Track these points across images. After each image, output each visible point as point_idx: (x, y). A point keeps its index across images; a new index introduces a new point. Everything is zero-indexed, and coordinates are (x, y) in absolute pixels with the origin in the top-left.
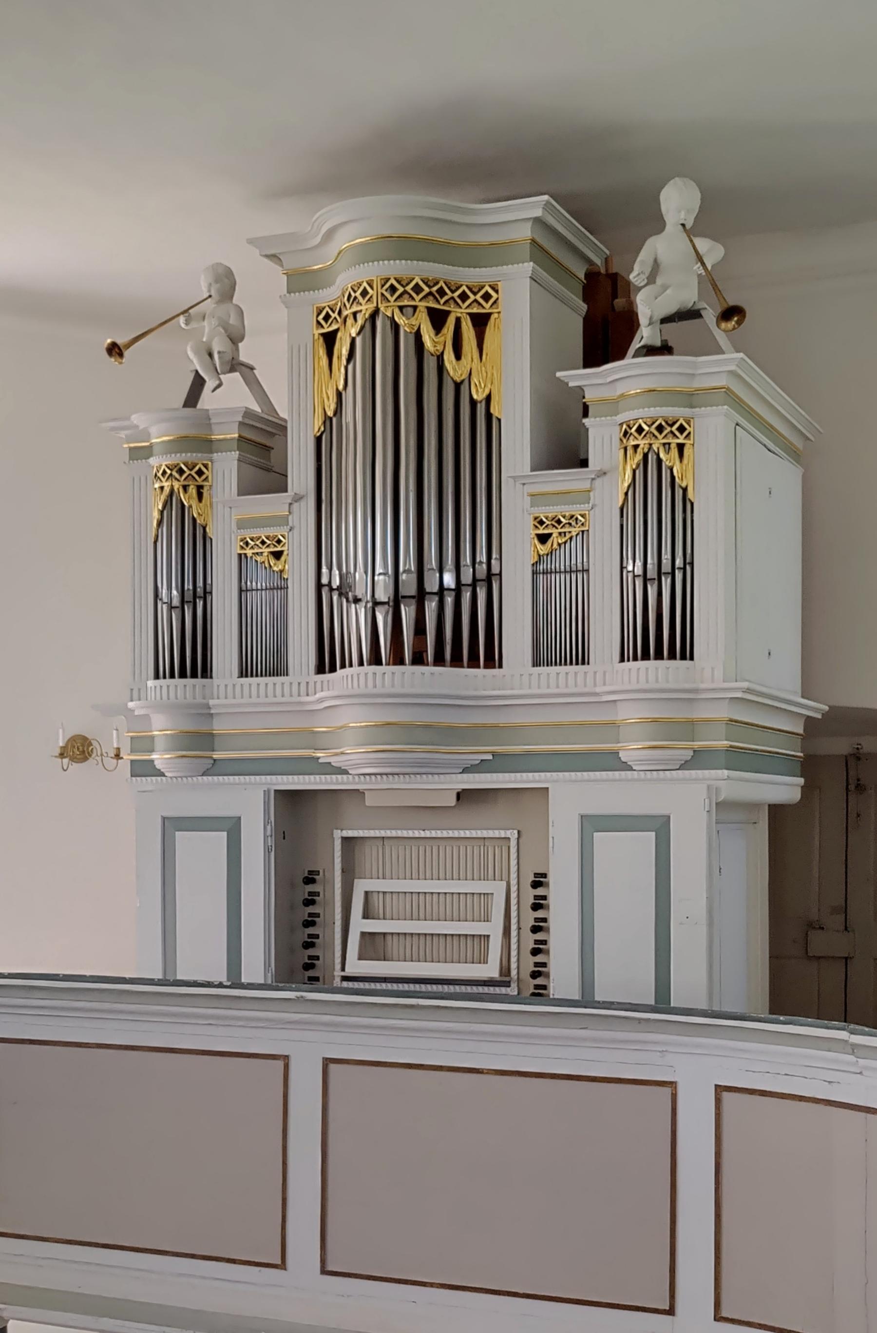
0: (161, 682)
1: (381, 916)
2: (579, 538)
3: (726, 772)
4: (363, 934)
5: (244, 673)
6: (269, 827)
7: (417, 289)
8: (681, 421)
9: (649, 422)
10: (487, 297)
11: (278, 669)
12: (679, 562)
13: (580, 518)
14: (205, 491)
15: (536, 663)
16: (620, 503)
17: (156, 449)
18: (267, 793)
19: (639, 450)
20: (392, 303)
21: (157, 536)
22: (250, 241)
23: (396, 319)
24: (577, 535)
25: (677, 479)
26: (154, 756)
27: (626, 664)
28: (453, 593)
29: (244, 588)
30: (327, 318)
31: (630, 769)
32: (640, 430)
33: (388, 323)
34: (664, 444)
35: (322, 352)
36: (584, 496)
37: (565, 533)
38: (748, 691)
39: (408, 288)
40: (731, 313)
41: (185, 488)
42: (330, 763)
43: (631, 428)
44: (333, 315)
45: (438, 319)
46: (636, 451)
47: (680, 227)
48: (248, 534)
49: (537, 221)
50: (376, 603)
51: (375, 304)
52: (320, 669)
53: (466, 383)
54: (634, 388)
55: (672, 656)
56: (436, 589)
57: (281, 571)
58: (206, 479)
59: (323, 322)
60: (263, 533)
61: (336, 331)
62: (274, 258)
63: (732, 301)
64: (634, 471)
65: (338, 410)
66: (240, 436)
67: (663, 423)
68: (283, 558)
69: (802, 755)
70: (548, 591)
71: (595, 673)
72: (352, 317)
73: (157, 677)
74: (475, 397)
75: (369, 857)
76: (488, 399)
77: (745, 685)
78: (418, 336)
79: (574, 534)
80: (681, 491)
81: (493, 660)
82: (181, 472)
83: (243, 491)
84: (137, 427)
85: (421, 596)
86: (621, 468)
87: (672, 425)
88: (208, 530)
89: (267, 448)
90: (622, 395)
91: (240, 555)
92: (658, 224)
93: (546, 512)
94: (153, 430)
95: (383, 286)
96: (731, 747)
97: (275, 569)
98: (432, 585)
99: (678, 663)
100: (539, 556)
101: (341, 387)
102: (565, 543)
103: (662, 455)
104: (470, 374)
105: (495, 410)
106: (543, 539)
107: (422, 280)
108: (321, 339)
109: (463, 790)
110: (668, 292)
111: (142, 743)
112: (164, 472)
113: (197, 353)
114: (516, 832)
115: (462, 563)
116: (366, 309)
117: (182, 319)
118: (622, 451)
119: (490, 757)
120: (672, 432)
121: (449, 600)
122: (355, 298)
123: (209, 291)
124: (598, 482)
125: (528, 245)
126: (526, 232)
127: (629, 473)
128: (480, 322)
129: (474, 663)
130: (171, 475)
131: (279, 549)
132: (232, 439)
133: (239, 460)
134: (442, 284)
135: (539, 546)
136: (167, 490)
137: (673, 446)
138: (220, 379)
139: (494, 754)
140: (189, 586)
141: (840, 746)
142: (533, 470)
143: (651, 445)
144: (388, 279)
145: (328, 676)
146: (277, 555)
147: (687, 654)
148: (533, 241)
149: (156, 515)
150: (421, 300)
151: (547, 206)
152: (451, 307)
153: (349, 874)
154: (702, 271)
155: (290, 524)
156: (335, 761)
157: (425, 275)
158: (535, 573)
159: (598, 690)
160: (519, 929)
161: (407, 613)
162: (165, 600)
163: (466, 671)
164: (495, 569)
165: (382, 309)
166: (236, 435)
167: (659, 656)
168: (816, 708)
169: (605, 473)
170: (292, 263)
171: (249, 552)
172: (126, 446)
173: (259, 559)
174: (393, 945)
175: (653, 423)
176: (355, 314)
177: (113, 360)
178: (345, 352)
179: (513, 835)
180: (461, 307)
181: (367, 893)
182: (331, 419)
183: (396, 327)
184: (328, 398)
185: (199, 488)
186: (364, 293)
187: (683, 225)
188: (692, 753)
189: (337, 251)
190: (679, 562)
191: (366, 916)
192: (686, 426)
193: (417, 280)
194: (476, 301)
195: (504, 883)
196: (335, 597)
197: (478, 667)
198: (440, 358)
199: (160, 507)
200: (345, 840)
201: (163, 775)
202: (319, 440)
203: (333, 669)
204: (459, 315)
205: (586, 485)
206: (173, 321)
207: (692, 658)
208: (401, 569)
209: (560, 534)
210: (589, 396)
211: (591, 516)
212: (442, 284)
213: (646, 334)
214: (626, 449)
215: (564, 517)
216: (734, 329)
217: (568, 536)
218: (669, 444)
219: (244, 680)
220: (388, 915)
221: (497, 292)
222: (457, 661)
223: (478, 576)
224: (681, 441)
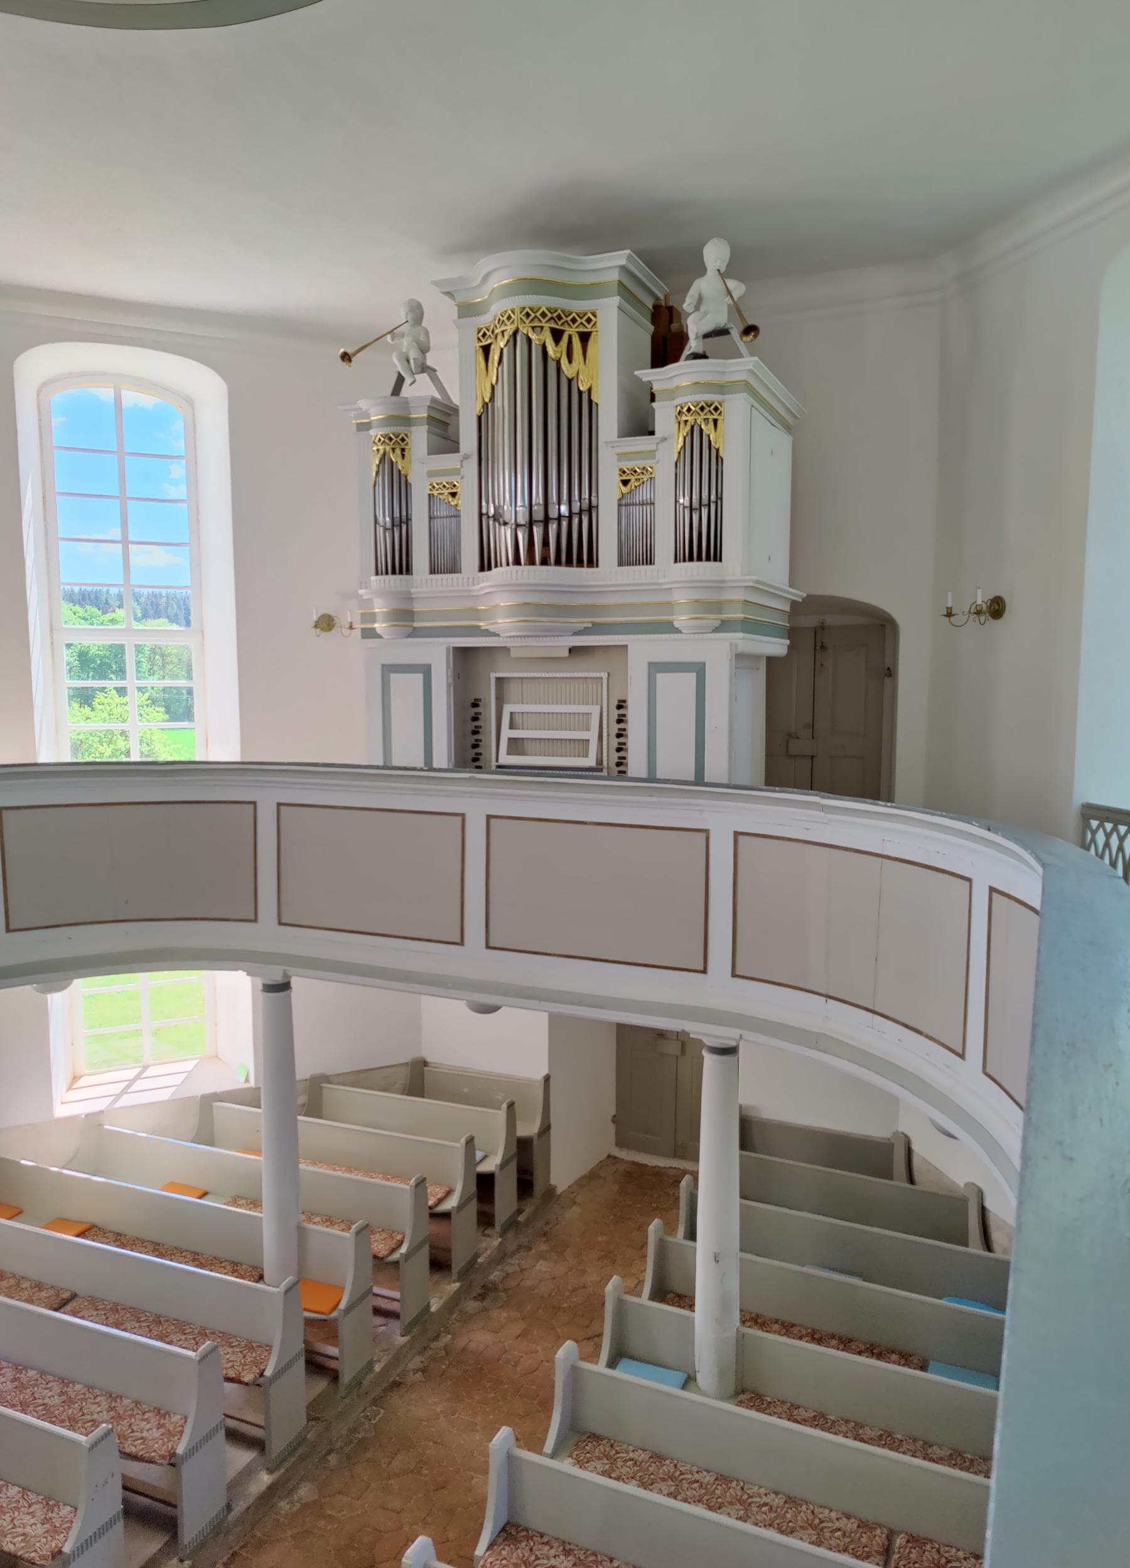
0: (380, 577)
1: (521, 727)
2: (649, 482)
3: (741, 635)
4: (510, 739)
5: (433, 571)
6: (449, 671)
7: (544, 315)
8: (716, 404)
9: (695, 404)
10: (589, 320)
11: (454, 568)
12: (713, 498)
13: (649, 469)
14: (406, 453)
15: (620, 564)
16: (675, 459)
17: (374, 424)
18: (448, 649)
19: (689, 424)
20: (527, 324)
21: (375, 482)
22: (435, 283)
23: (530, 335)
24: (647, 480)
25: (712, 443)
26: (376, 625)
27: (678, 564)
28: (567, 519)
29: (432, 516)
30: (484, 335)
31: (680, 632)
32: (689, 410)
33: (525, 337)
34: (705, 419)
36: (652, 454)
37: (639, 479)
38: (757, 582)
39: (538, 314)
40: (750, 330)
41: (393, 450)
42: (487, 630)
43: (682, 408)
44: (488, 333)
45: (557, 335)
46: (686, 424)
47: (717, 272)
48: (435, 481)
49: (623, 268)
50: (518, 525)
51: (516, 325)
53: (575, 380)
54: (685, 382)
55: (708, 559)
56: (556, 516)
57: (456, 505)
58: (407, 444)
59: (481, 338)
60: (444, 480)
61: (490, 345)
62: (449, 294)
63: (751, 322)
64: (685, 438)
65: (492, 398)
66: (428, 416)
67: (705, 405)
68: (457, 497)
69: (788, 625)
70: (628, 517)
71: (658, 571)
72: (501, 334)
73: (377, 574)
74: (581, 388)
75: (512, 690)
76: (590, 390)
77: (754, 578)
78: (544, 347)
79: (645, 480)
80: (715, 451)
81: (592, 562)
82: (391, 439)
83: (429, 454)
84: (361, 409)
85: (546, 521)
86: (676, 436)
87: (709, 406)
88: (408, 478)
89: (446, 424)
90: (677, 387)
91: (429, 495)
92: (702, 270)
93: (627, 465)
94: (372, 411)
95: (521, 313)
96: (746, 618)
97: (452, 503)
98: (553, 514)
99: (712, 564)
100: (623, 494)
101: (494, 382)
102: (639, 486)
103: (703, 427)
104: (578, 373)
105: (594, 398)
106: (625, 483)
107: (547, 309)
108: (481, 350)
109: (574, 647)
110: (709, 316)
111: (370, 617)
112: (380, 440)
113: (399, 359)
114: (606, 674)
115: (573, 499)
116: (510, 329)
117: (389, 337)
118: (677, 424)
119: (590, 625)
120: (710, 411)
121: (565, 524)
122: (503, 321)
123: (406, 318)
124: (661, 445)
125: (616, 285)
126: (614, 276)
127: (681, 439)
128: (585, 337)
129: (580, 563)
130: (384, 441)
131: (454, 491)
132: (424, 417)
133: (428, 432)
134: (559, 311)
135: (623, 488)
136: (382, 452)
137: (711, 421)
138: (414, 377)
139: (594, 624)
140: (397, 514)
141: (809, 621)
142: (619, 437)
143: (696, 420)
144: (524, 308)
145: (486, 573)
146: (454, 495)
147: (717, 557)
148: (620, 282)
149: (375, 468)
150: (546, 322)
151: (629, 258)
152: (566, 328)
153: (500, 701)
154: (731, 302)
155: (462, 474)
156: (492, 628)
157: (549, 305)
158: (620, 505)
159: (661, 581)
160: (608, 735)
161: (537, 532)
163: (574, 571)
164: (594, 503)
165: (521, 329)
166: (426, 415)
167: (700, 559)
168: (798, 595)
169: (665, 439)
170: (461, 298)
171: (435, 493)
172: (354, 422)
173: (441, 497)
174: (529, 746)
175: (698, 405)
176: (503, 332)
177: (345, 364)
178: (496, 358)
179: (604, 675)
180: (571, 327)
181: (511, 713)
182: (487, 404)
183: (529, 341)
184: (485, 389)
185: (403, 450)
186: (509, 318)
187: (719, 270)
188: (719, 622)
189: (491, 289)
190: (713, 498)
191: (512, 726)
192: (719, 407)
193: (544, 309)
194: (582, 323)
195: (599, 707)
196: (491, 523)
197: (583, 566)
198: (558, 362)
199: (377, 462)
200: (499, 680)
202: (480, 418)
203: (490, 568)
204: (570, 333)
205: (653, 447)
206: (384, 338)
207: (721, 560)
208: (534, 503)
209: (636, 479)
210: (656, 388)
212: (559, 311)
213: (693, 345)
214: (679, 423)
215: (639, 468)
216: (752, 341)
217: (641, 481)
218: (708, 419)
220: (525, 727)
221: (595, 316)
222: (569, 563)
223: (583, 508)
224: (715, 417)
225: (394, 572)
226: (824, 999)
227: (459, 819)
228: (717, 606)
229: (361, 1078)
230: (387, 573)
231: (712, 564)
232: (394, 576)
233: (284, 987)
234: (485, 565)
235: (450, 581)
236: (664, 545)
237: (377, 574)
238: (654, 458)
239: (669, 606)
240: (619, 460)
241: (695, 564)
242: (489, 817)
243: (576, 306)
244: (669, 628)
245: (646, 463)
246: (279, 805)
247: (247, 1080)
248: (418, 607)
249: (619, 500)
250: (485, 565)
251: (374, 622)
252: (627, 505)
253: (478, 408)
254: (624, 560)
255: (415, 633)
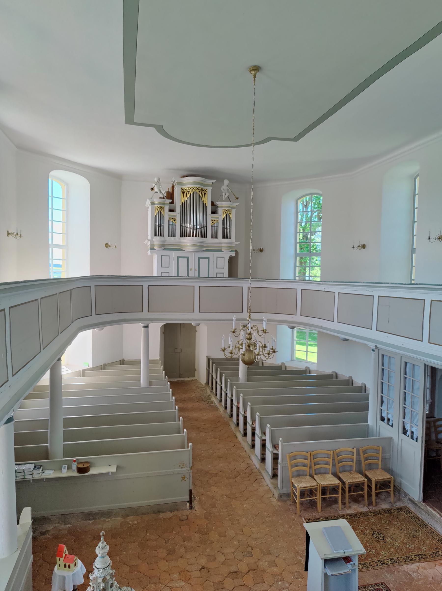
0: (156, 237)
5: (169, 236)
10: (206, 191)
31: (223, 252)
35: (182, 194)
45: (201, 192)
48: (170, 217)
52: (181, 237)
63: (237, 197)
68: (175, 221)
73: (155, 236)
74: (204, 203)
76: (205, 204)
85: (196, 229)
93: (212, 219)
103: (229, 214)
105: (206, 205)
106: (213, 222)
118: (223, 213)
127: (224, 215)
128: (205, 194)
139: (206, 249)
146: (175, 221)
156: (183, 249)
158: (211, 227)
162: (189, 227)
167: (228, 238)
183: (197, 193)
185: (163, 210)
201: (156, 250)
202: (181, 206)
203: (182, 237)
211: (219, 220)
214: (224, 213)
219: (169, 237)
221: (207, 190)
225: (160, 236)
226: (265, 314)
227: (193, 287)
228: (231, 247)
229: (112, 364)
230: (158, 236)
231: (230, 239)
232: (160, 237)
233: (147, 327)
234: (182, 236)
235: (175, 239)
236: (220, 235)
237: (155, 236)
238: (218, 218)
239: (221, 247)
240: (211, 218)
241: (227, 239)
242: (200, 286)
243: (204, 188)
244: (221, 251)
245: (217, 219)
246: (149, 285)
247: (88, 367)
248: (165, 243)
249: (211, 226)
250: (182, 236)
251: (154, 246)
252: (212, 227)
253: (181, 204)
254: (212, 237)
255: (165, 249)
